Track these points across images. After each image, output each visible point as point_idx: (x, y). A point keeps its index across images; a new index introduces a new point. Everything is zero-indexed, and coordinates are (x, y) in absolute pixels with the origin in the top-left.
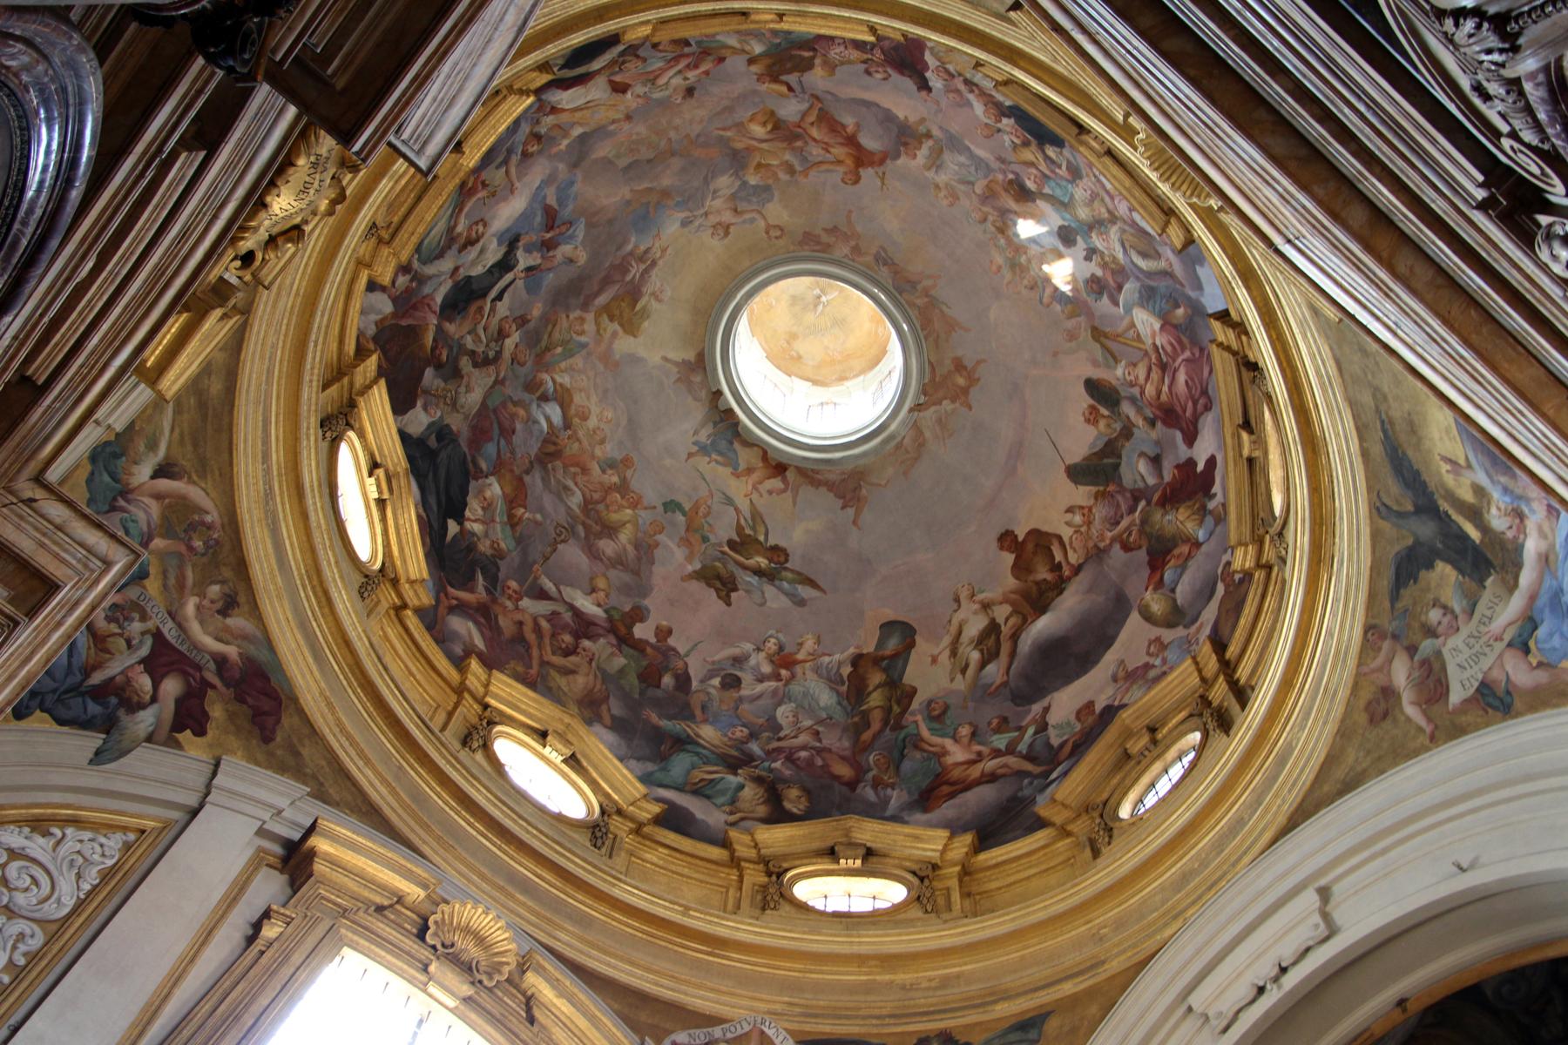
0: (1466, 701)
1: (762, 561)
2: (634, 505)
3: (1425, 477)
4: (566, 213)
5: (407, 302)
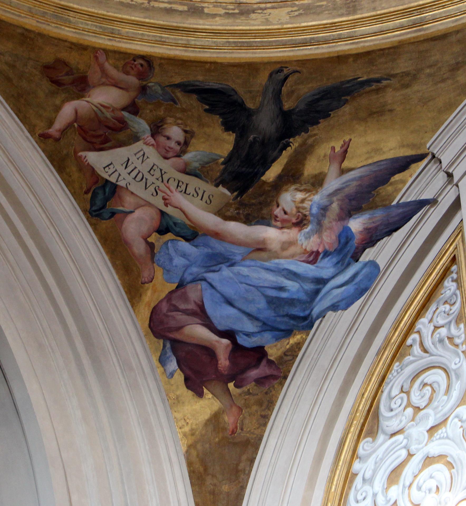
3: (323, 123)
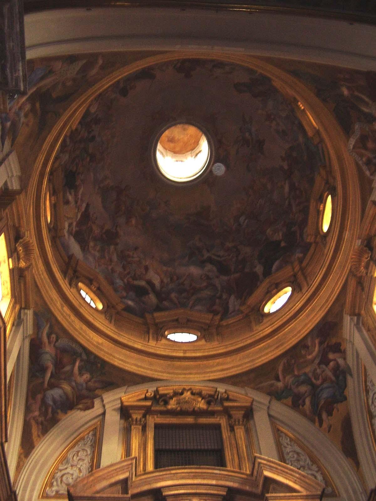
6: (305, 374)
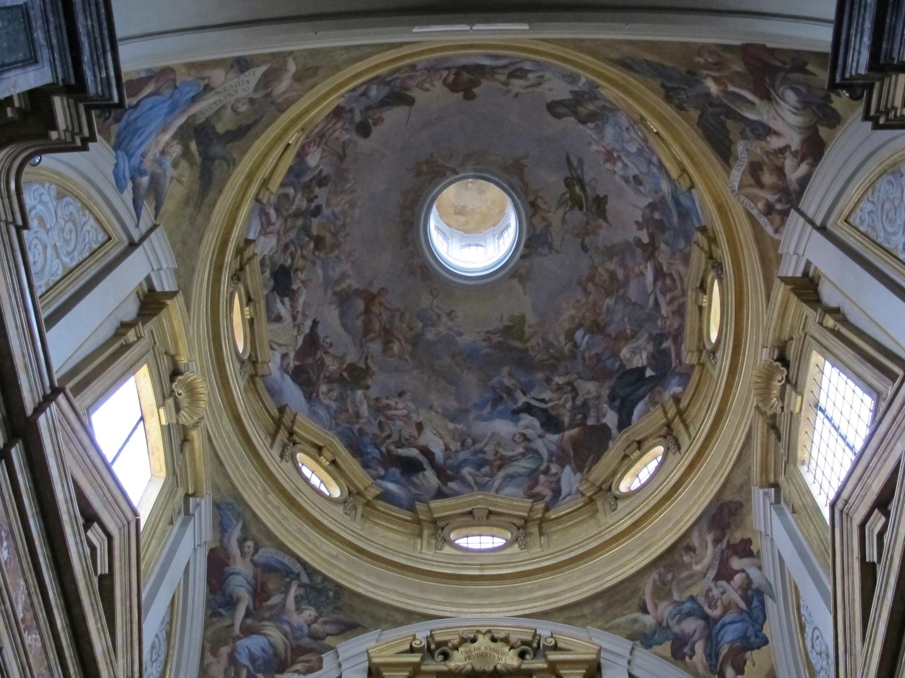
0: (258, 66)
1: (577, 189)
2: (594, 268)
4: (489, 395)
5: (562, 458)
6: (692, 599)
